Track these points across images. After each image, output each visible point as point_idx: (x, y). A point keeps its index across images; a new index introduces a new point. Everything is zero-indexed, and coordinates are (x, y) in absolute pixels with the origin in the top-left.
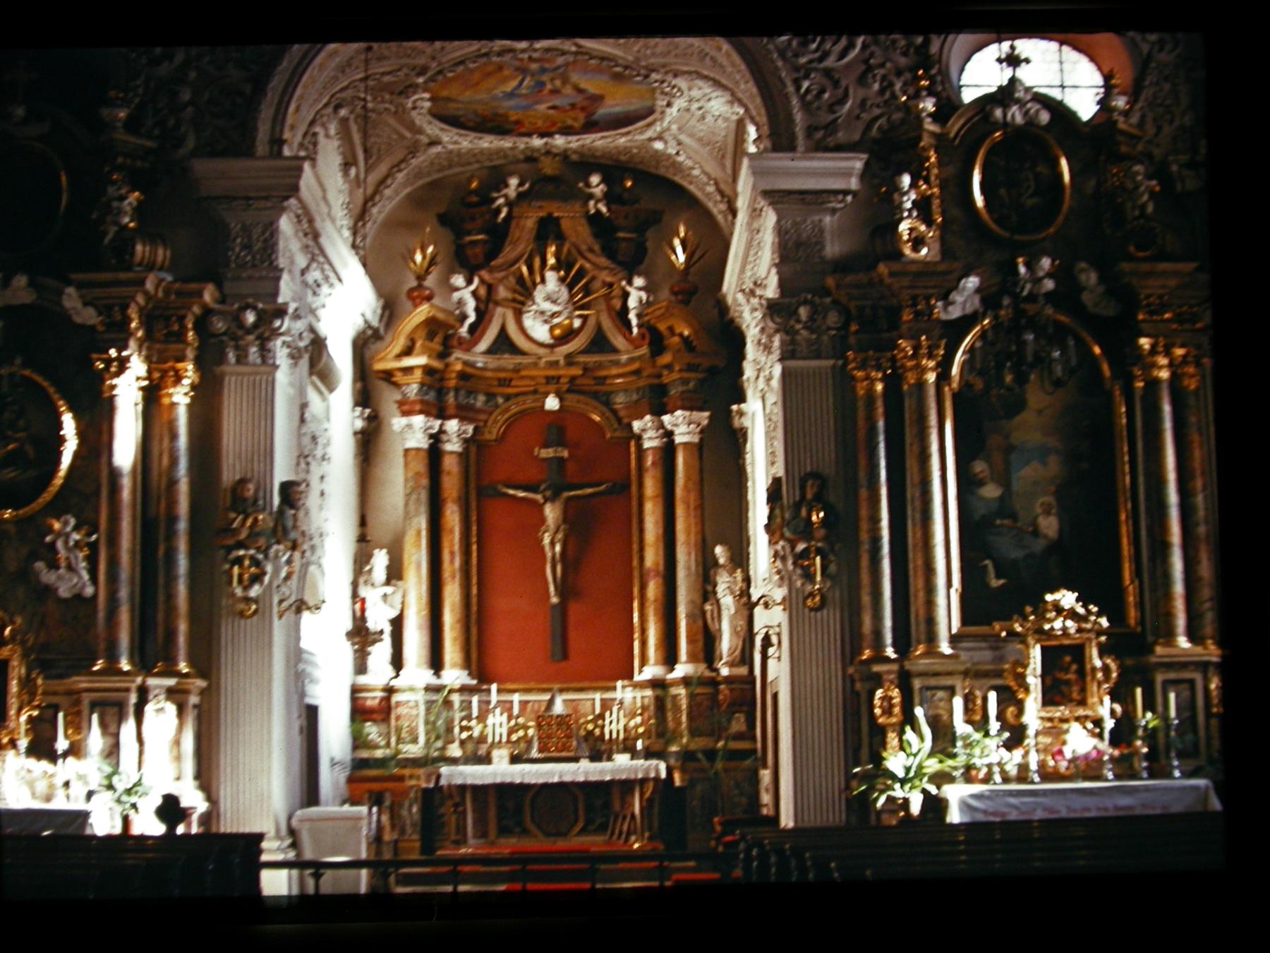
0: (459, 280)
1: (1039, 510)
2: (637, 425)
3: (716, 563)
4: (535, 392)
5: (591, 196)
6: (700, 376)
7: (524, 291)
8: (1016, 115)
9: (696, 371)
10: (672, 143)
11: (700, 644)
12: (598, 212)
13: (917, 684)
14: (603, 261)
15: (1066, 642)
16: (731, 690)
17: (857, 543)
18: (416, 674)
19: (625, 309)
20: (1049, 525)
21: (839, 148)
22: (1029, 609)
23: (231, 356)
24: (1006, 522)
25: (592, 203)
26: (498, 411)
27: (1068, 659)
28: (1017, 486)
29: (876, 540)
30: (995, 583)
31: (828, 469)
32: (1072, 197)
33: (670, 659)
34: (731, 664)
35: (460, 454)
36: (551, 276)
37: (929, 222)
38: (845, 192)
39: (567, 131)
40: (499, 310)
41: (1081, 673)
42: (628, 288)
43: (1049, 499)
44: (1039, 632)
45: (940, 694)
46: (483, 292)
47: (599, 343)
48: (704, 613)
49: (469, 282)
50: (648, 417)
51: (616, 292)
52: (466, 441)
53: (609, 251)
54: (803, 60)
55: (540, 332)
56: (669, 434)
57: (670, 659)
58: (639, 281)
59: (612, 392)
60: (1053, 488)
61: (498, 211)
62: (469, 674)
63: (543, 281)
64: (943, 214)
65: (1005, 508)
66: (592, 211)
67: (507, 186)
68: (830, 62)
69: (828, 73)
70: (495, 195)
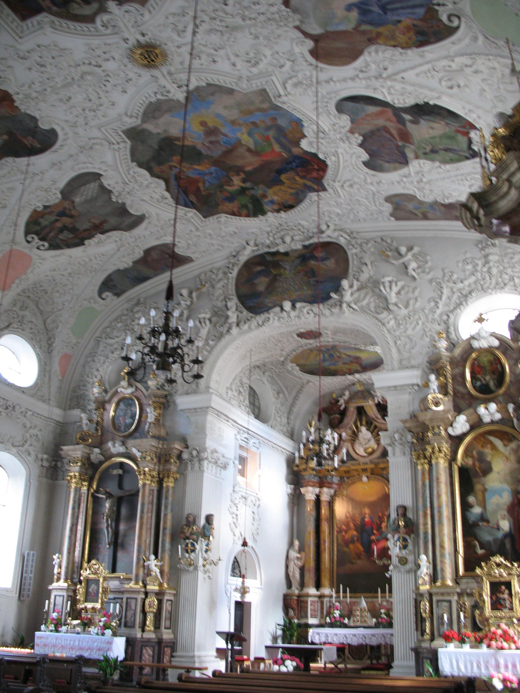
1: (499, 517)
5: (376, 396)
7: (354, 436)
8: (483, 344)
13: (434, 599)
15: (502, 580)
17: (418, 535)
20: (505, 525)
21: (413, 367)
22: (483, 564)
23: (189, 468)
24: (485, 524)
27: (503, 587)
28: (489, 507)
29: (426, 533)
30: (480, 552)
31: (408, 502)
32: (510, 376)
36: (363, 429)
37: (446, 394)
38: (413, 385)
39: (358, 372)
40: (346, 444)
41: (510, 595)
43: (506, 513)
44: (489, 575)
45: (445, 604)
54: (397, 333)
55: (361, 451)
60: (506, 507)
61: (341, 406)
64: (454, 389)
65: (483, 518)
66: (376, 401)
67: (344, 395)
68: (409, 332)
69: (408, 337)
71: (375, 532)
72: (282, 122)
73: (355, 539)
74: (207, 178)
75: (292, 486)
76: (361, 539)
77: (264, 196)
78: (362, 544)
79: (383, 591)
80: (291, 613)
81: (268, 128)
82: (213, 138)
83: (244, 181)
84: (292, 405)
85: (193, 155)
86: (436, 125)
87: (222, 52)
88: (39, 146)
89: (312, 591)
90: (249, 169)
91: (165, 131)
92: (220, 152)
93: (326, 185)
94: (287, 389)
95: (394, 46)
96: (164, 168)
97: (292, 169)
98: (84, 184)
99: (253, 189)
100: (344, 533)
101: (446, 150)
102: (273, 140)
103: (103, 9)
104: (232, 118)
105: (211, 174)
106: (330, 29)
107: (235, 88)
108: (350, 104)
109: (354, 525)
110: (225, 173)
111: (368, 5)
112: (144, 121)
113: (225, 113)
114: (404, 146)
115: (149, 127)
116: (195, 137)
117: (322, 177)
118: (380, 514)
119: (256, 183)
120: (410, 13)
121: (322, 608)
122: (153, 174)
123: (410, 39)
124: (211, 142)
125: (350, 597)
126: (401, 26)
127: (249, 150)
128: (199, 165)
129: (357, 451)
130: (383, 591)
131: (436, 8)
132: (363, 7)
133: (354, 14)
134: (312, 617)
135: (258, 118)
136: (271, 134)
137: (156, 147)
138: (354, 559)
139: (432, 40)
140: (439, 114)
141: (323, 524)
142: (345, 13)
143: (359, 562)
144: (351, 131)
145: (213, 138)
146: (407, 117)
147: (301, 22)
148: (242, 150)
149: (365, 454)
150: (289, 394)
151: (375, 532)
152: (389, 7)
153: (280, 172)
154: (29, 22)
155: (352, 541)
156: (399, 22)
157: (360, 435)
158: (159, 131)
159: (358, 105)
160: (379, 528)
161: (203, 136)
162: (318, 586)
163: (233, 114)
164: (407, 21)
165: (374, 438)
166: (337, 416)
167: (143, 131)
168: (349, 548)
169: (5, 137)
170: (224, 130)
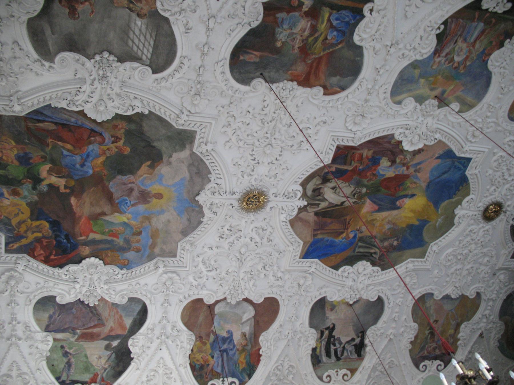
72: (130, 255)
74: (78, 159)
77: (15, 193)
81: (127, 241)
82: (135, 193)
83: (51, 186)
85: (121, 166)
86: (103, 361)
87: (226, 246)
88: (241, 58)
90: (73, 201)
91: (170, 163)
92: (112, 190)
93: (20, 255)
95: (192, 350)
96: (121, 133)
97: (57, 236)
98: (156, 47)
99: (34, 188)
101: (69, 364)
102: (109, 238)
103: (304, 195)
104: (154, 221)
105: (83, 165)
106: (216, 318)
107: (187, 238)
108: (138, 308)
110: (77, 178)
111: (229, 343)
112: (193, 154)
113: (163, 218)
114: (75, 334)
115: (184, 154)
116: (143, 178)
117: (34, 257)
119: (41, 195)
120: (218, 364)
122: (118, 116)
123: (198, 360)
124: (131, 190)
126: (210, 358)
127: (104, 214)
128: (103, 163)
131: (222, 379)
132: (228, 340)
133: (225, 334)
135: (145, 239)
136: (120, 241)
137: (155, 144)
139: (196, 373)
140: (118, 365)
142: (227, 329)
144: (102, 300)
145: (135, 193)
146: (115, 343)
147: (228, 303)
148: (107, 209)
152: (225, 354)
153: (55, 225)
154: (334, 149)
156: (213, 357)
158: (173, 159)
159: (135, 313)
161: (143, 188)
163: (158, 223)
164: (212, 362)
167: (183, 147)
169: (279, 44)
170: (141, 208)
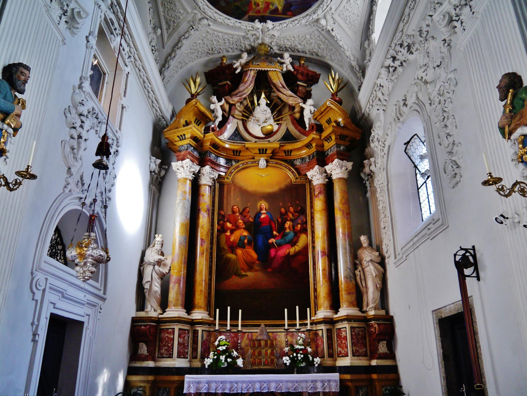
0: (214, 99)
2: (309, 174)
3: (359, 245)
4: (254, 158)
6: (347, 143)
9: (344, 140)
10: (331, 21)
11: (354, 296)
12: (289, 72)
14: (290, 93)
16: (378, 324)
18: (175, 311)
19: (302, 116)
25: (285, 65)
26: (232, 168)
33: (335, 306)
34: (375, 309)
35: (210, 186)
36: (263, 101)
42: (304, 106)
46: (227, 107)
47: (288, 137)
48: (355, 275)
49: (219, 100)
50: (317, 167)
51: (297, 109)
52: (214, 180)
53: (294, 88)
55: (257, 131)
56: (329, 177)
57: (335, 306)
58: (310, 102)
59: (294, 160)
61: (236, 69)
62: (209, 314)
63: (259, 105)
66: (285, 69)
70: (235, 62)
71: (275, 233)
73: (246, 241)
75: (159, 161)
76: (253, 243)
78: (255, 250)
79: (292, 317)
80: (144, 349)
84: (170, 55)
89: (181, 313)
94: (169, 27)
100: (228, 233)
109: (244, 223)
118: (283, 210)
121: (195, 342)
125: (242, 326)
129: (251, 131)
130: (292, 317)
134: (179, 356)
138: (243, 269)
141: (201, 216)
143: (250, 274)
149: (262, 136)
150: (169, 36)
151: (275, 233)
155: (241, 244)
157: (257, 109)
160: (281, 229)
162: (189, 305)
165: (274, 118)
166: (229, 83)
168: (236, 255)
